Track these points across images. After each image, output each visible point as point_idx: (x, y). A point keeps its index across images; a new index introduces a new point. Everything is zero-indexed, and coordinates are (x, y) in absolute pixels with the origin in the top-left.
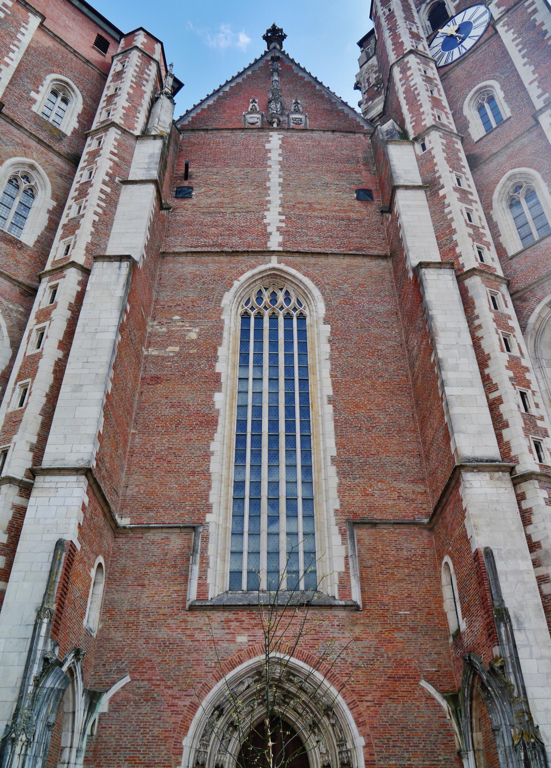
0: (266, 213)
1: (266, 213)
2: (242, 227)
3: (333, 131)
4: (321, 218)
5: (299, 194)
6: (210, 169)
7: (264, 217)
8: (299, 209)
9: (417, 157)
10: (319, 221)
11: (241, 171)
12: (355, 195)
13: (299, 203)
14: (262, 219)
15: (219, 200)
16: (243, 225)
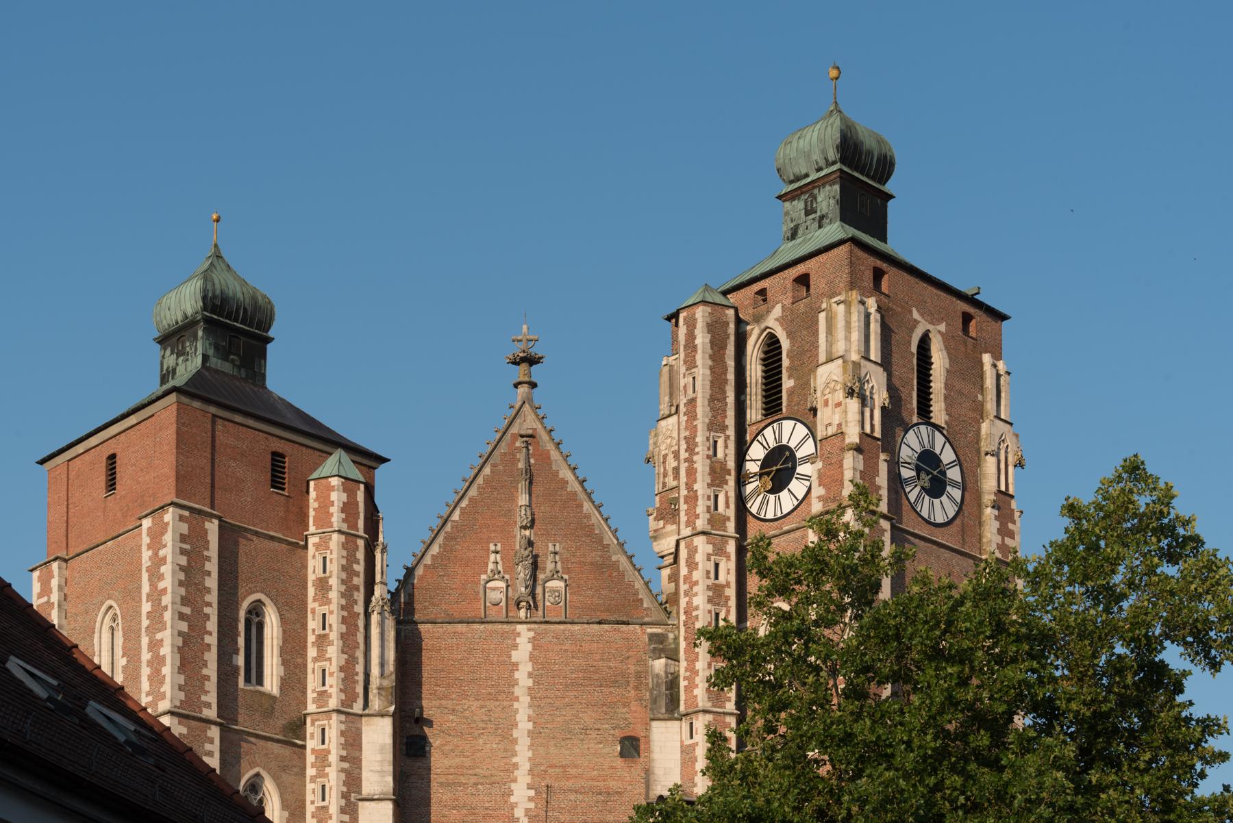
0: (513, 786)
1: (513, 786)
2: (486, 809)
3: (600, 623)
4: (576, 791)
5: (552, 750)
6: (444, 702)
7: (511, 793)
8: (551, 776)
9: (682, 742)
10: (572, 797)
11: (482, 707)
12: (619, 748)
13: (551, 766)
14: (509, 796)
15: (458, 761)
16: (487, 805)
